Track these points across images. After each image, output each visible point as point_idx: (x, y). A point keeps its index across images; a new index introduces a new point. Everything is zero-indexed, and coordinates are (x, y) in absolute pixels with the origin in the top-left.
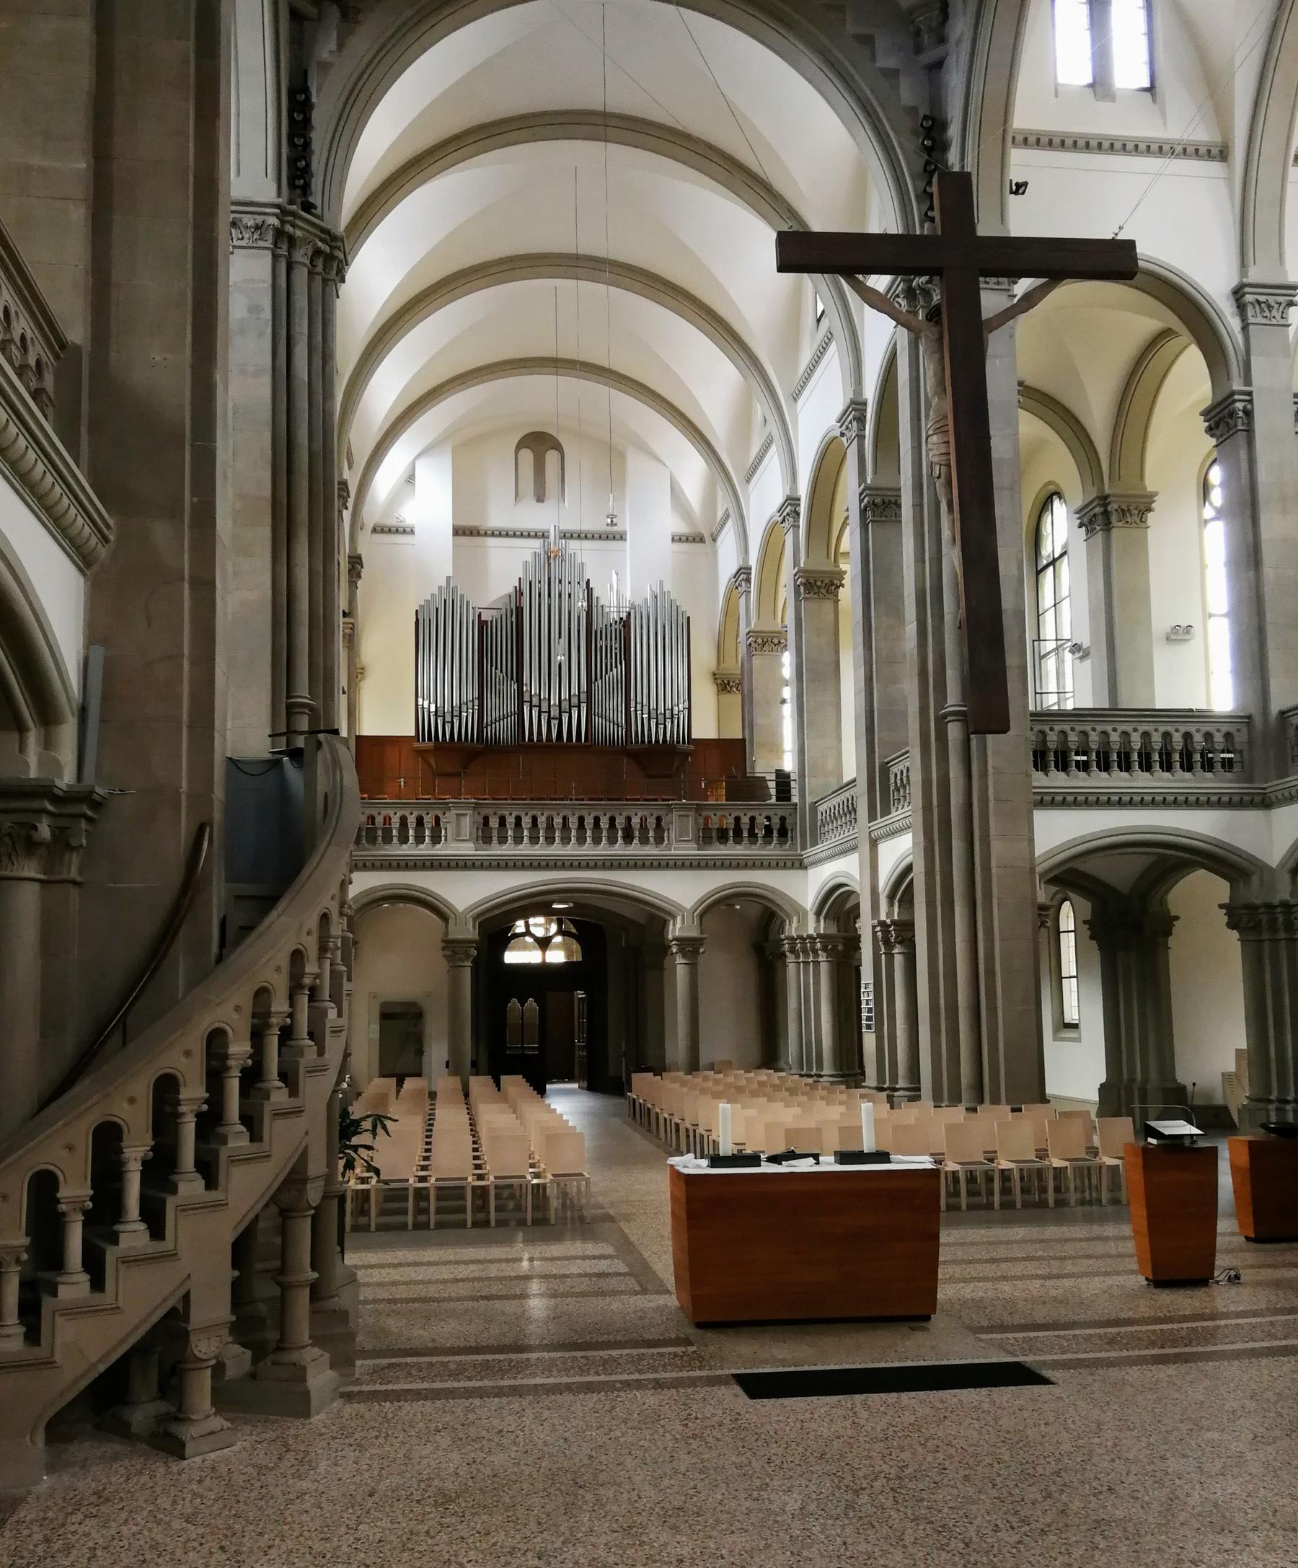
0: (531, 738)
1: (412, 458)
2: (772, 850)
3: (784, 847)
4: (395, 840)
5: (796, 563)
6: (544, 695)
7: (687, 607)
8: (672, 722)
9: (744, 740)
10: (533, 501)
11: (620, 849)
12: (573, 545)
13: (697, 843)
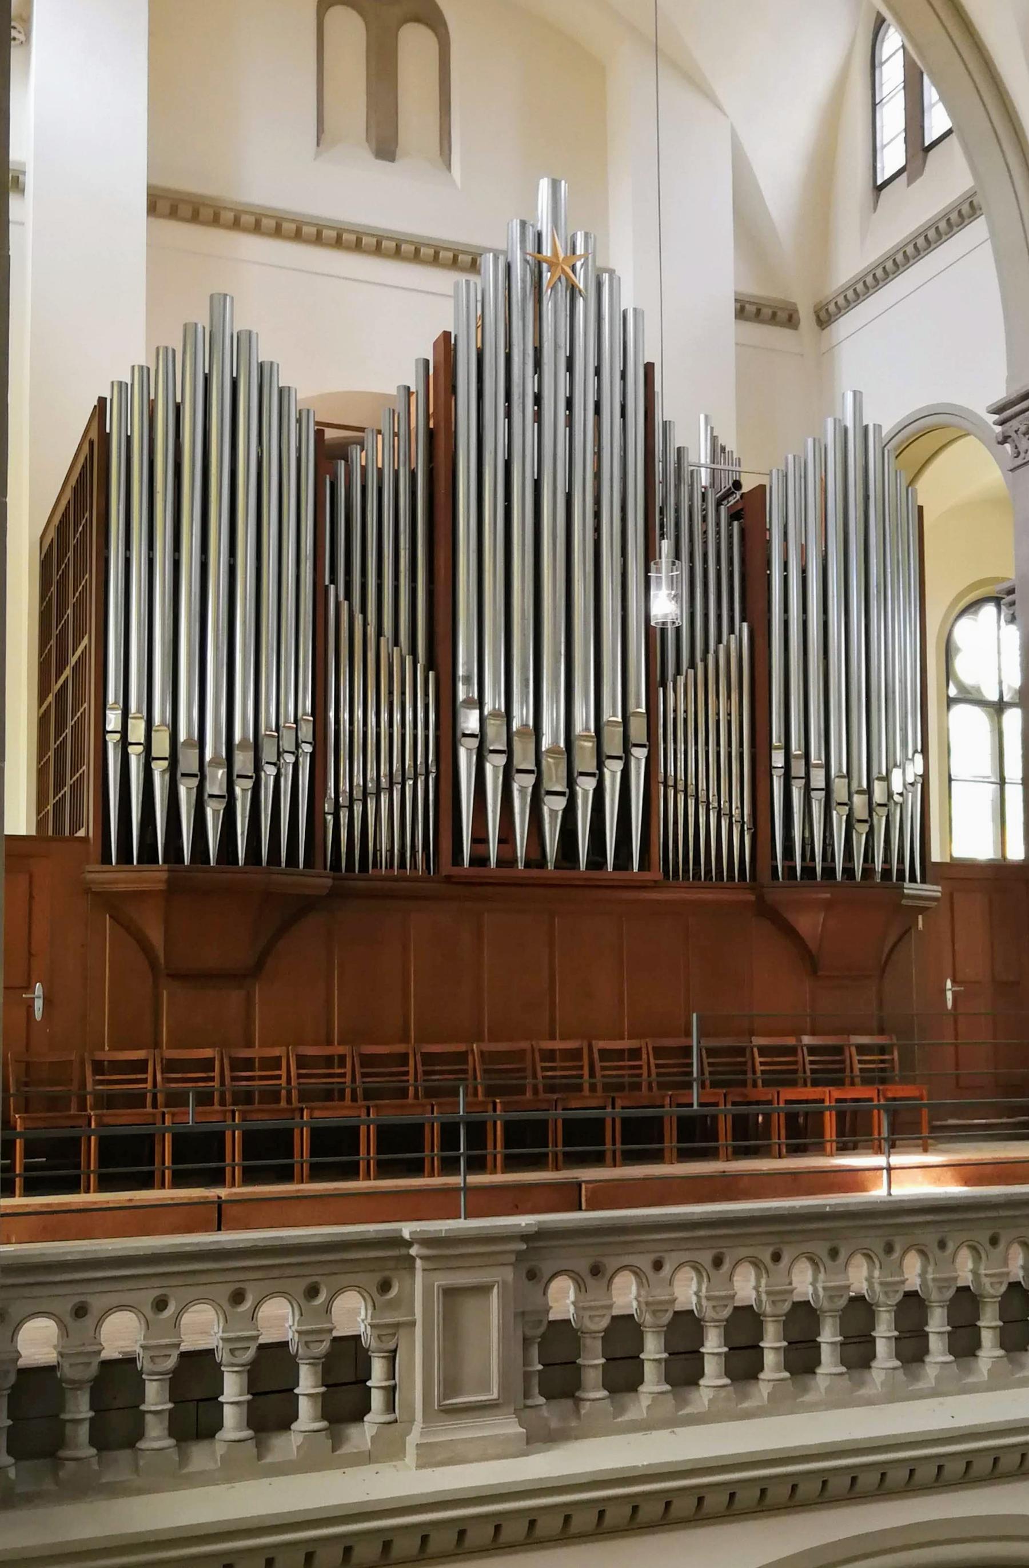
6: (522, 714)
10: (366, 154)
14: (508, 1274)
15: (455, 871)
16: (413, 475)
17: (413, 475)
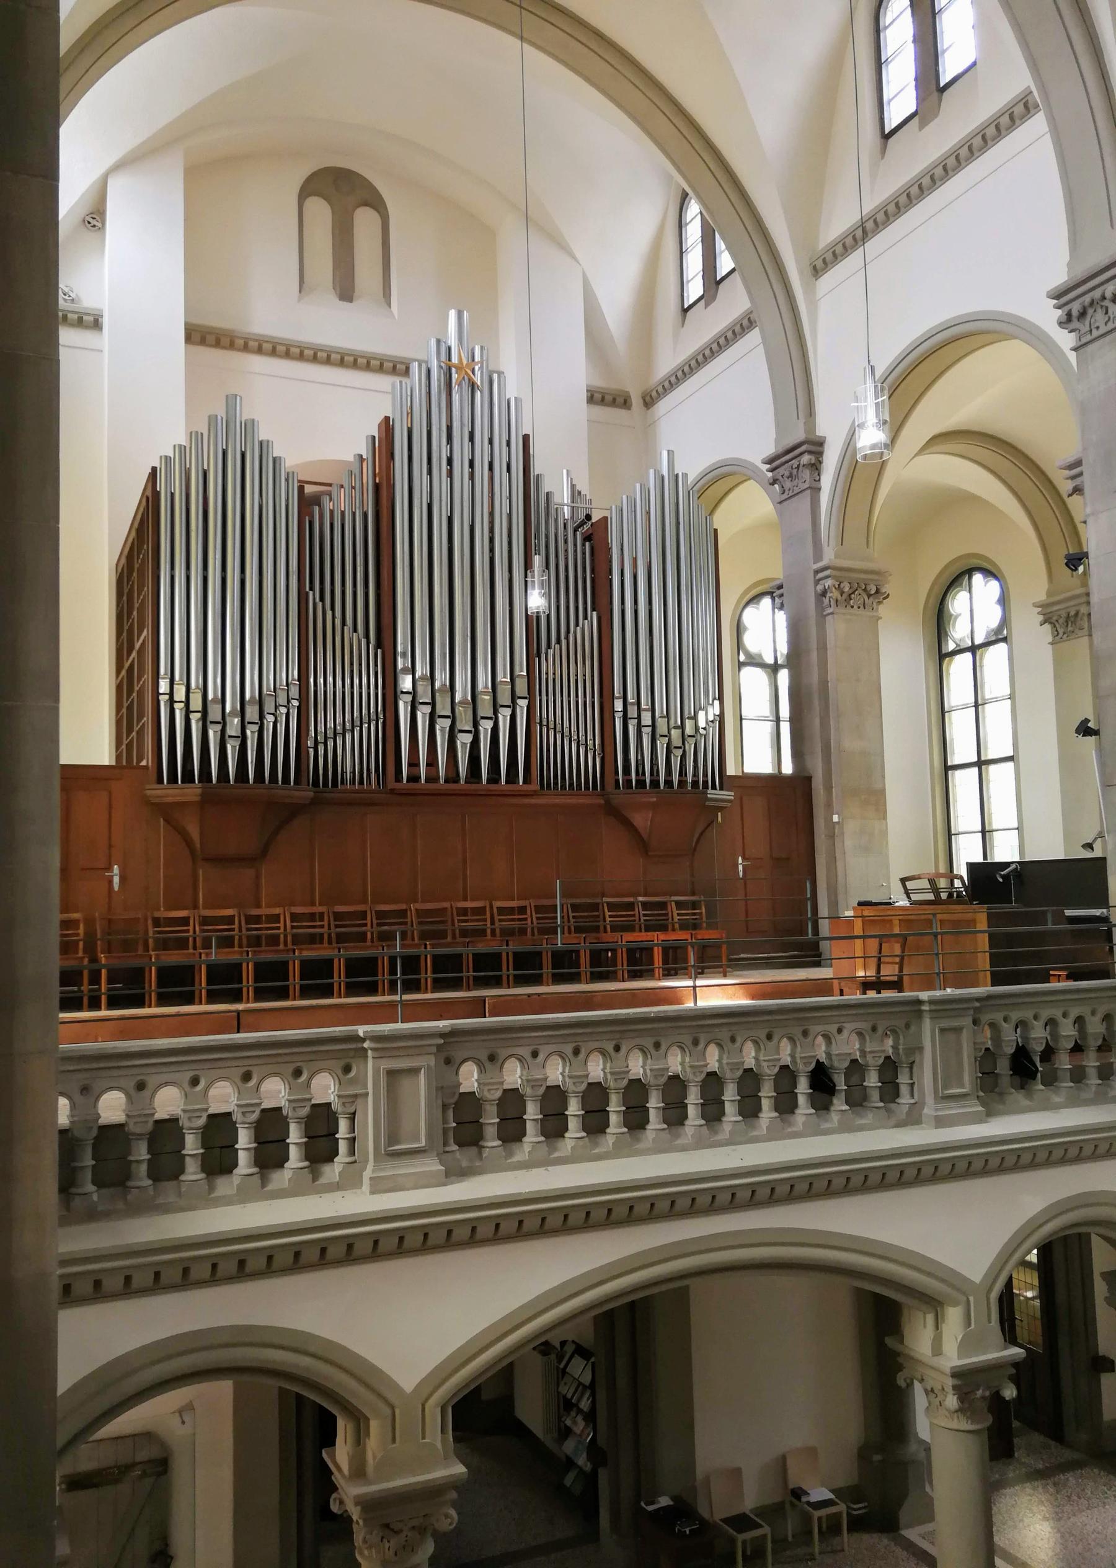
6: (441, 678)
14: (431, 1061)
15: (398, 786)
16: (365, 515)
17: (365, 515)
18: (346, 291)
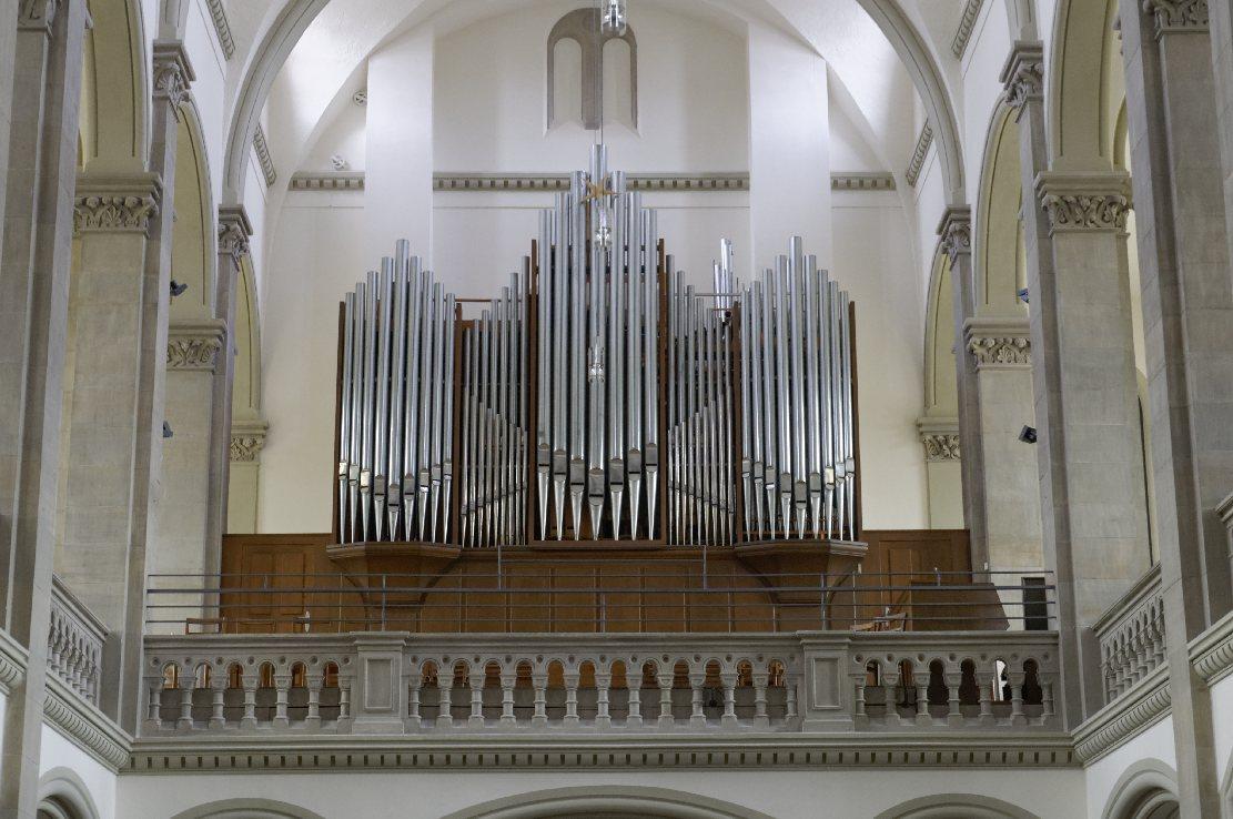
0: (551, 536)
1: (357, 60)
2: (1014, 729)
3: (1033, 723)
4: (250, 713)
5: (1039, 163)
7: (849, 285)
8: (823, 499)
9: (966, 532)
11: (698, 728)
12: (649, 199)
13: (855, 717)
16: (519, 323)
17: (519, 323)
18: (593, 121)
